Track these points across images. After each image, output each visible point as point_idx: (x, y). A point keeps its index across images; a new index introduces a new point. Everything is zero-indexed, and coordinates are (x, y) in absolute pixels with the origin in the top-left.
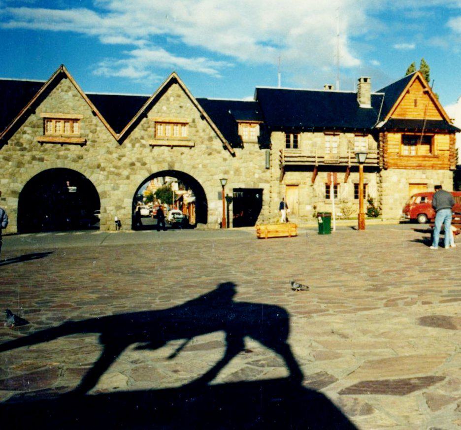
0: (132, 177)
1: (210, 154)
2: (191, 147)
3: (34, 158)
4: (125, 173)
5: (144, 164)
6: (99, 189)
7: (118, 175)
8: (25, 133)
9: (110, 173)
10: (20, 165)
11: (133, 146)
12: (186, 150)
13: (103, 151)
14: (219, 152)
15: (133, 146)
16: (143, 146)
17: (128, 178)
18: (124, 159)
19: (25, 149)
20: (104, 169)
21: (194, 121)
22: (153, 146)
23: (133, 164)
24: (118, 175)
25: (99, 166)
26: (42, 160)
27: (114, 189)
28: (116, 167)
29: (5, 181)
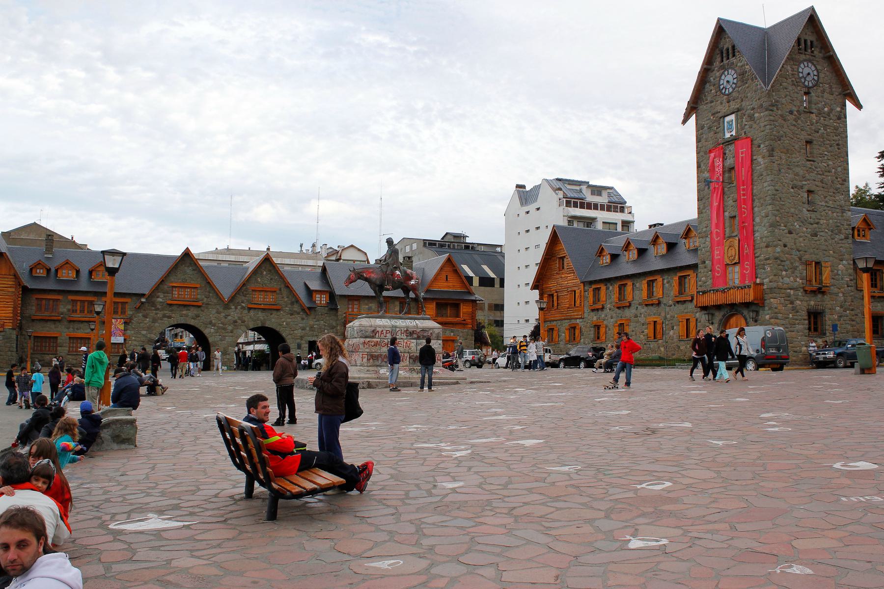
0: (235, 331)
1: (292, 314)
2: (278, 310)
3: (164, 316)
4: (230, 328)
5: (243, 322)
6: (210, 340)
7: (224, 329)
8: (158, 297)
9: (219, 328)
10: (154, 320)
11: (236, 308)
12: (275, 312)
13: (214, 311)
14: (298, 313)
15: (236, 308)
16: (243, 308)
17: (232, 332)
18: (229, 318)
19: (158, 309)
20: (214, 325)
21: (280, 290)
22: (250, 309)
23: (235, 322)
24: (224, 329)
25: (211, 323)
26: (170, 317)
27: (221, 340)
28: (222, 323)
29: (144, 332)
